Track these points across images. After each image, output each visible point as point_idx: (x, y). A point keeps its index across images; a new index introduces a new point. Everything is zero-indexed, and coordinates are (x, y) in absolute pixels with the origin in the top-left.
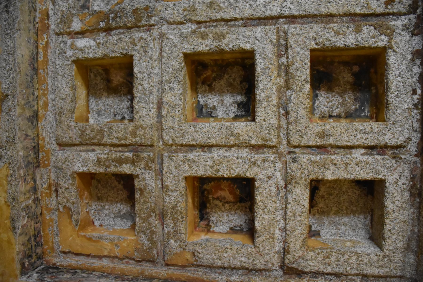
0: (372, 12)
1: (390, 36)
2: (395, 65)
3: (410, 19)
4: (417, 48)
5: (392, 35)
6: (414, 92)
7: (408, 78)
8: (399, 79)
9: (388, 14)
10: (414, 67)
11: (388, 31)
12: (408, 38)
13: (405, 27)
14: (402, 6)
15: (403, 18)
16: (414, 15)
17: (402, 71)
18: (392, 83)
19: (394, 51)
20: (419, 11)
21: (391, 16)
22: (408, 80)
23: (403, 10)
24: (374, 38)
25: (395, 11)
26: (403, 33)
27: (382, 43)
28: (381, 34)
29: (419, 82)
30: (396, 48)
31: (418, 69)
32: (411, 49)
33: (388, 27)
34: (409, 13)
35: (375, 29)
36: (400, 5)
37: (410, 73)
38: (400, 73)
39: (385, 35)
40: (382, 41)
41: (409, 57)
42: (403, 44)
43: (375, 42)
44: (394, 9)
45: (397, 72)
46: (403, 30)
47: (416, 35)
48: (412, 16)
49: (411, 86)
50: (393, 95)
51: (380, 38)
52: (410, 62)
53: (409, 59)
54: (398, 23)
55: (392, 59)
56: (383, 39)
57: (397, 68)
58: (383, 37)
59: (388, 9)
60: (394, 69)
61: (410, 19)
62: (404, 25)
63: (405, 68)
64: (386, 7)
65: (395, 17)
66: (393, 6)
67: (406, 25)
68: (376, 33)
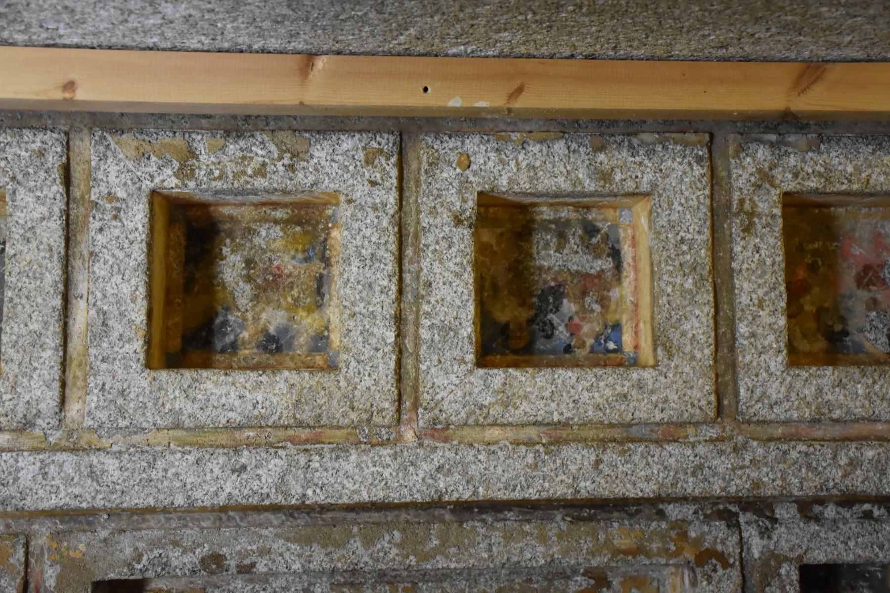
0: (739, 590)
1: (781, 559)
2: (829, 550)
3: (747, 523)
4: (796, 511)
5: (778, 556)
6: (868, 515)
7: (850, 528)
8: (851, 544)
9: (741, 559)
10: (826, 515)
11: (773, 564)
12: (783, 529)
13: (765, 533)
14: (730, 539)
15: (745, 535)
16: (741, 515)
17: (838, 539)
18: (860, 556)
19: (805, 554)
20: (734, 508)
21: (743, 555)
22: (854, 529)
23: (735, 538)
24: (784, 586)
25: (738, 551)
26: (775, 538)
27: (792, 573)
28: (779, 575)
29: (851, 507)
30: (800, 550)
31: (829, 509)
32: (802, 524)
33: (765, 563)
34: (738, 525)
35: (769, 585)
36: (728, 543)
37: (841, 526)
38: (842, 542)
39: (780, 568)
40: (789, 572)
41: (814, 527)
42: (794, 538)
43: (792, 585)
44: (734, 552)
45: (841, 546)
46: (769, 538)
47: (773, 511)
48: (742, 519)
49: (862, 524)
50: (881, 555)
51: (784, 578)
52: (822, 526)
53: (817, 528)
54: (757, 546)
55: (819, 556)
56: (786, 570)
57: (833, 548)
58: (783, 571)
59: (734, 563)
60: (836, 553)
61: (747, 523)
62: (762, 535)
63: (833, 534)
64: (732, 566)
65: (745, 547)
66: (729, 555)
67: (761, 533)
68: (775, 582)
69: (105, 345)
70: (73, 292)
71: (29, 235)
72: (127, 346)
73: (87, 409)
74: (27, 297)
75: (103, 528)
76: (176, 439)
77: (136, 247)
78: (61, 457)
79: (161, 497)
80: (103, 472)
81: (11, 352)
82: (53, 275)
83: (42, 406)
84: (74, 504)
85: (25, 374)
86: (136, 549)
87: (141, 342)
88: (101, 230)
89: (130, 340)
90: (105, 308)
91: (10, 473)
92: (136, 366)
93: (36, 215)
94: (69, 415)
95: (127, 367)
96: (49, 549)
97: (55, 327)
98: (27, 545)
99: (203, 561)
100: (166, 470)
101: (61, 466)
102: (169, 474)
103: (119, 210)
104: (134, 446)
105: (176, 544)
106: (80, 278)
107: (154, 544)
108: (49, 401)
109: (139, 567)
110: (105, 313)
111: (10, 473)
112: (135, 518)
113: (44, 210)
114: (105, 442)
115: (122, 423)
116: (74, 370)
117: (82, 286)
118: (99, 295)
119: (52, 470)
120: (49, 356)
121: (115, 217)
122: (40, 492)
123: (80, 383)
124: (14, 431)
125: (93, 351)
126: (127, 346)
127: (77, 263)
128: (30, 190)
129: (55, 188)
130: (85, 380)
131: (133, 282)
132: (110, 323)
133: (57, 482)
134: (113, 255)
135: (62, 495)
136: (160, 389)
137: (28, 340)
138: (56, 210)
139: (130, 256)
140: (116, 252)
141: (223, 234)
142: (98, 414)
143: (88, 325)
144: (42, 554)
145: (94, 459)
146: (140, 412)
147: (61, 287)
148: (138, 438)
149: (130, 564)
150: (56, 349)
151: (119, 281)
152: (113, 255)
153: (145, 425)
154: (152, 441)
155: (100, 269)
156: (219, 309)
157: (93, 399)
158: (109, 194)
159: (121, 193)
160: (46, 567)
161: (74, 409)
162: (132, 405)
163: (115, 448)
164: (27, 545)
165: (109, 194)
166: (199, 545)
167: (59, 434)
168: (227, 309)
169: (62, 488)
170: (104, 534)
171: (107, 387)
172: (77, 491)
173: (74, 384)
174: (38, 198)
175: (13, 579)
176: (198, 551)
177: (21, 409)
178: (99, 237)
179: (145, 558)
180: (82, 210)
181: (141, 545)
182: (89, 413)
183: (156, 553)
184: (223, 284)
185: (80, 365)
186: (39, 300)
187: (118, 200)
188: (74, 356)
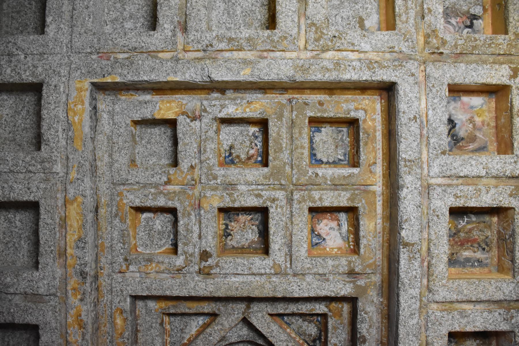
69: (458, 317)
70: (476, 303)
71: (498, 288)
72: (457, 325)
73: (435, 311)
74: (475, 289)
75: (377, 299)
76: (422, 343)
77: (494, 327)
78: (418, 303)
79: (403, 340)
80: (412, 318)
81: (457, 284)
82: (483, 297)
83: (437, 296)
84: (401, 309)
85: (448, 289)
86: (369, 312)
87: (459, 330)
88: (500, 314)
89: (459, 326)
90: (471, 316)
91: (413, 286)
92: (450, 329)
93: (505, 291)
94: (432, 304)
95: (450, 325)
96: (371, 282)
97: (465, 299)
98: (372, 273)
99: (364, 336)
100: (412, 341)
101: (415, 303)
102: (410, 342)
103: (507, 320)
104: (420, 328)
105: (370, 326)
106: (481, 306)
107: (371, 319)
108: (437, 298)
109: (363, 313)
110: (469, 316)
111: (413, 286)
112: (380, 311)
113: (507, 293)
114: (422, 318)
115: (429, 324)
116: (448, 306)
117: (478, 307)
118: (476, 314)
119: (414, 300)
120: (455, 297)
121: (504, 319)
122: (406, 297)
123: (444, 307)
124: (428, 286)
125: (456, 313)
126: (457, 325)
127: (486, 305)
128: (514, 289)
129: (515, 297)
130: (445, 310)
131: (481, 326)
132: (466, 318)
133: (409, 302)
134: (490, 319)
135: (405, 305)
136: (442, 338)
137: (461, 290)
138: (507, 298)
139: (490, 324)
140: (492, 320)
141: (484, 340)
142: (433, 315)
143: (465, 310)
144: (369, 278)
145: (417, 315)
146: (434, 331)
147: (480, 300)
148: (423, 329)
149: (364, 310)
150: (457, 300)
151: (481, 321)
152: (490, 319)
153: (428, 332)
154: (422, 334)
155: (485, 314)
156: (456, 340)
157: (438, 314)
158: (513, 317)
159: (513, 321)
160: (364, 280)
161: (434, 306)
162: (436, 328)
163: (420, 321)
164: (372, 273)
165: (513, 317)
166: (369, 335)
167: (426, 301)
168: (456, 343)
169: (407, 304)
170: (375, 300)
171: (443, 318)
172: (406, 310)
173: (443, 306)
174: (511, 291)
175: (361, 270)
176: (367, 334)
177: (436, 288)
178: (497, 314)
179: (366, 315)
180: (506, 306)
181: (371, 314)
182: (433, 312)
183: (368, 319)
184: (466, 341)
185: (450, 307)
186: (475, 293)
187: (511, 320)
188: (453, 305)
